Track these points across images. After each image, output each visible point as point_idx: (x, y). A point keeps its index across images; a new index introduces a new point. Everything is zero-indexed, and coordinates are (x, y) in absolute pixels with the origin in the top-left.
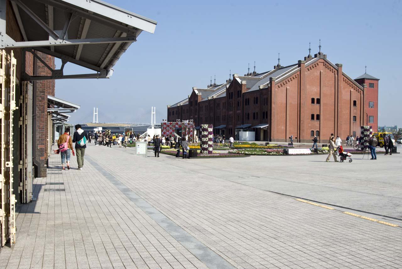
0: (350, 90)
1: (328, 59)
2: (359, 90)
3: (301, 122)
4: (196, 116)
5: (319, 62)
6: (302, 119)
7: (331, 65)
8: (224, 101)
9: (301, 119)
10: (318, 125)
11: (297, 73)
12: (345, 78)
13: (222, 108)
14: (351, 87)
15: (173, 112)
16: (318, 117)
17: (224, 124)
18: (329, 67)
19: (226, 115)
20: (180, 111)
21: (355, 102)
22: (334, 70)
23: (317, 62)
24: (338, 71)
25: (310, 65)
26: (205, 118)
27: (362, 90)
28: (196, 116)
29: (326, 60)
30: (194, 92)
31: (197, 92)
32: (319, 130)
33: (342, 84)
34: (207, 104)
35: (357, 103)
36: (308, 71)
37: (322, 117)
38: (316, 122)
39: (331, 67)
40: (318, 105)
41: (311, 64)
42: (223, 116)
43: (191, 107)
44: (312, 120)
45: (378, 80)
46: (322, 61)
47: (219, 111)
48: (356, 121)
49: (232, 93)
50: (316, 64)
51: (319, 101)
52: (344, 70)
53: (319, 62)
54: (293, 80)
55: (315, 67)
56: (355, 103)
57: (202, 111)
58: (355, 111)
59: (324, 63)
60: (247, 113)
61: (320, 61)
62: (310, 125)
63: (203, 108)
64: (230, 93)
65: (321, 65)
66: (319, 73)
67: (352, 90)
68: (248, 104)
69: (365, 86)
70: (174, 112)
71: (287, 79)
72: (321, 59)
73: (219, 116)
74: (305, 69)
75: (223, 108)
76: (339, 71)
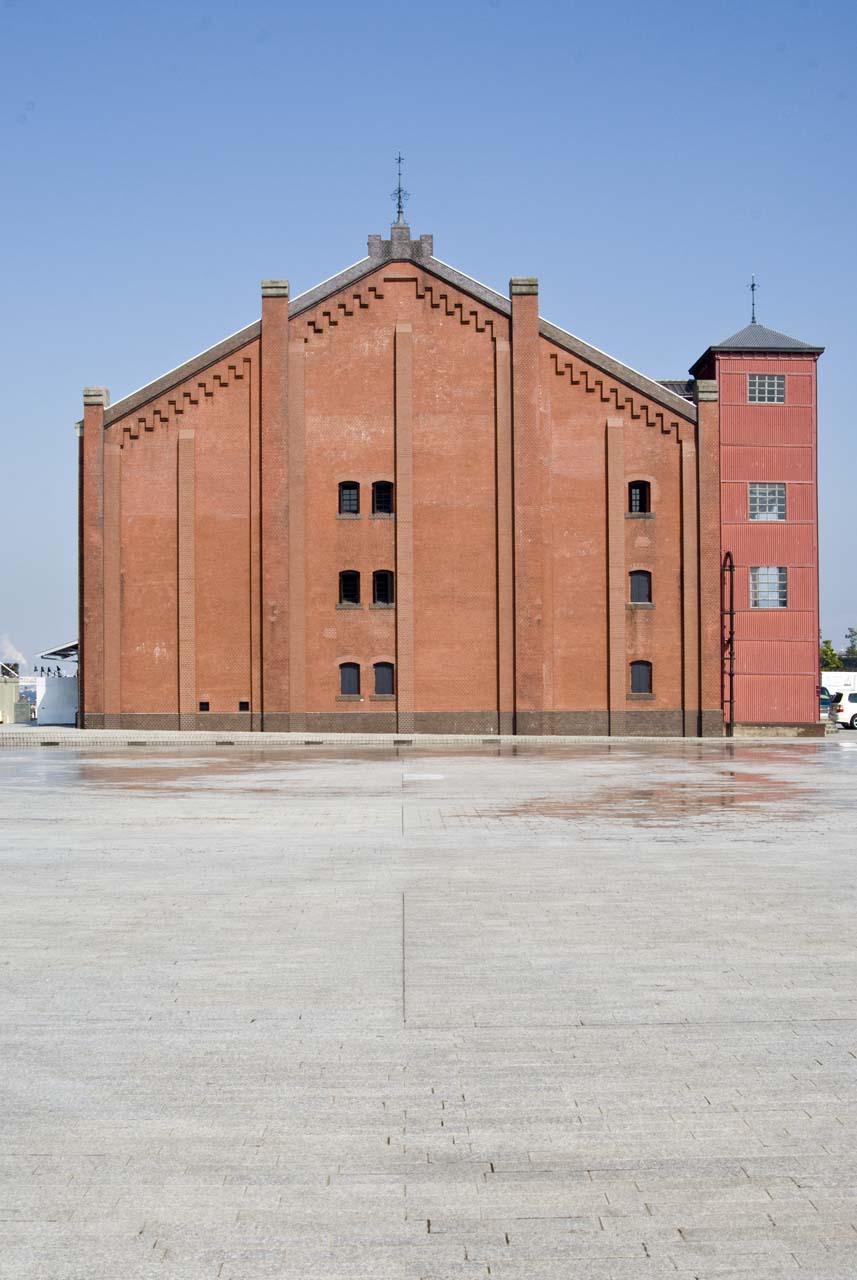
0: (601, 421)
1: (441, 259)
2: (669, 418)
3: (269, 618)
5: (386, 280)
6: (272, 603)
7: (465, 287)
9: (269, 602)
10: (388, 633)
11: (242, 354)
12: (562, 354)
14: (611, 405)
16: (385, 587)
18: (452, 301)
21: (640, 494)
22: (485, 315)
23: (370, 282)
24: (509, 318)
25: (323, 300)
27: (689, 420)
29: (428, 267)
32: (391, 660)
33: (544, 394)
35: (655, 494)
36: (312, 335)
37: (404, 587)
38: (369, 616)
39: (466, 301)
40: (383, 519)
41: (331, 295)
44: (345, 603)
45: (814, 353)
46: (408, 271)
48: (650, 600)
50: (363, 290)
51: (384, 496)
52: (550, 312)
53: (386, 280)
54: (219, 393)
55: (358, 311)
56: (640, 494)
58: (642, 541)
59: (415, 280)
61: (392, 276)
62: (330, 633)
65: (401, 298)
66: (387, 342)
67: (616, 421)
69: (701, 396)
71: (183, 389)
72: (394, 261)
74: (297, 322)
76: (515, 322)
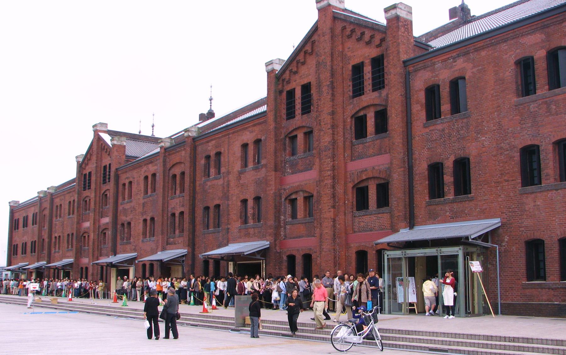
4: (106, 220)
8: (248, 137)
13: (238, 166)
15: (26, 219)
17: (246, 236)
19: (271, 190)
20: (47, 212)
26: (145, 220)
28: (106, 220)
30: (98, 140)
31: (107, 138)
34: (156, 168)
42: (245, 202)
43: (87, 193)
47: (220, 182)
49: (306, 88)
57: (130, 196)
60: (449, 165)
63: (134, 186)
64: (291, 94)
68: (456, 108)
70: (27, 216)
73: (218, 206)
75: (245, 165)
